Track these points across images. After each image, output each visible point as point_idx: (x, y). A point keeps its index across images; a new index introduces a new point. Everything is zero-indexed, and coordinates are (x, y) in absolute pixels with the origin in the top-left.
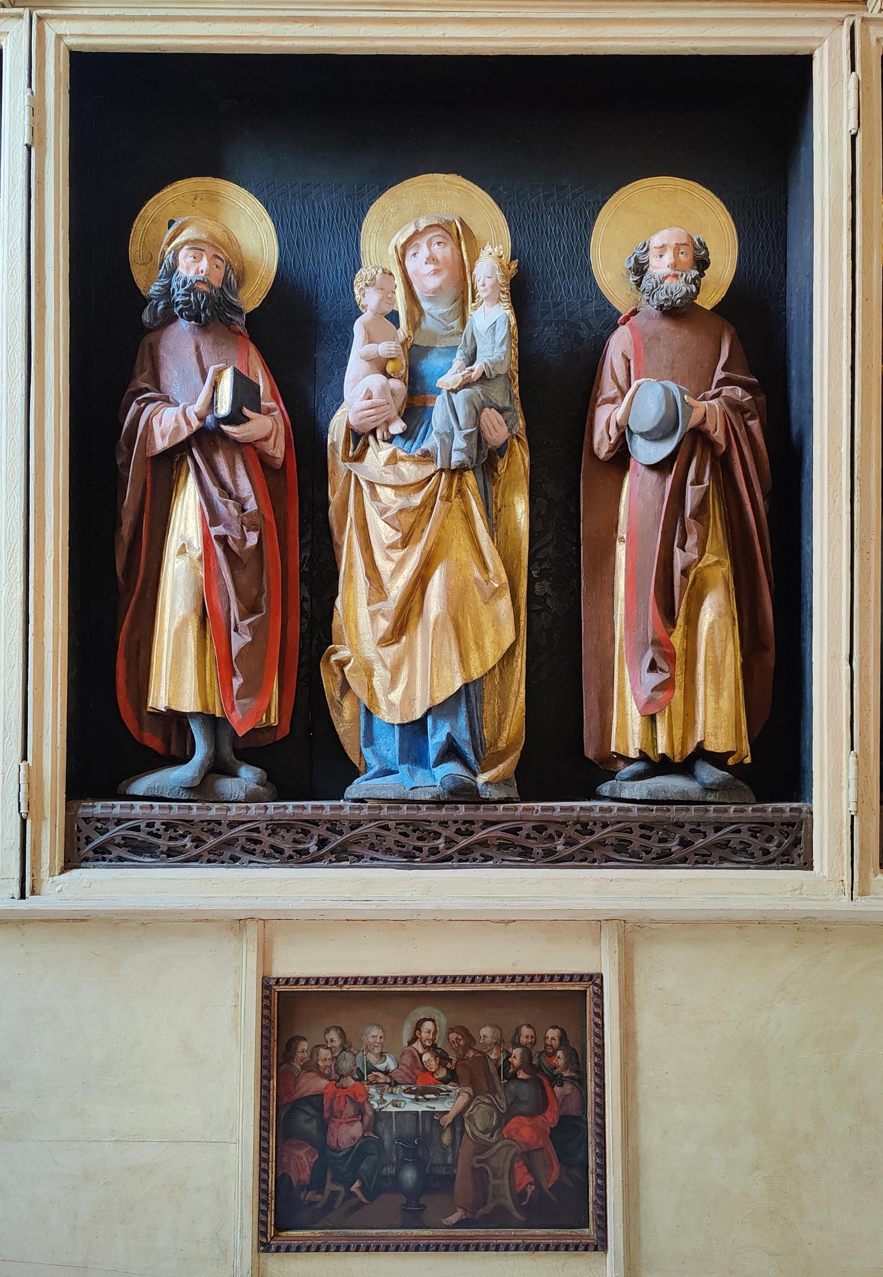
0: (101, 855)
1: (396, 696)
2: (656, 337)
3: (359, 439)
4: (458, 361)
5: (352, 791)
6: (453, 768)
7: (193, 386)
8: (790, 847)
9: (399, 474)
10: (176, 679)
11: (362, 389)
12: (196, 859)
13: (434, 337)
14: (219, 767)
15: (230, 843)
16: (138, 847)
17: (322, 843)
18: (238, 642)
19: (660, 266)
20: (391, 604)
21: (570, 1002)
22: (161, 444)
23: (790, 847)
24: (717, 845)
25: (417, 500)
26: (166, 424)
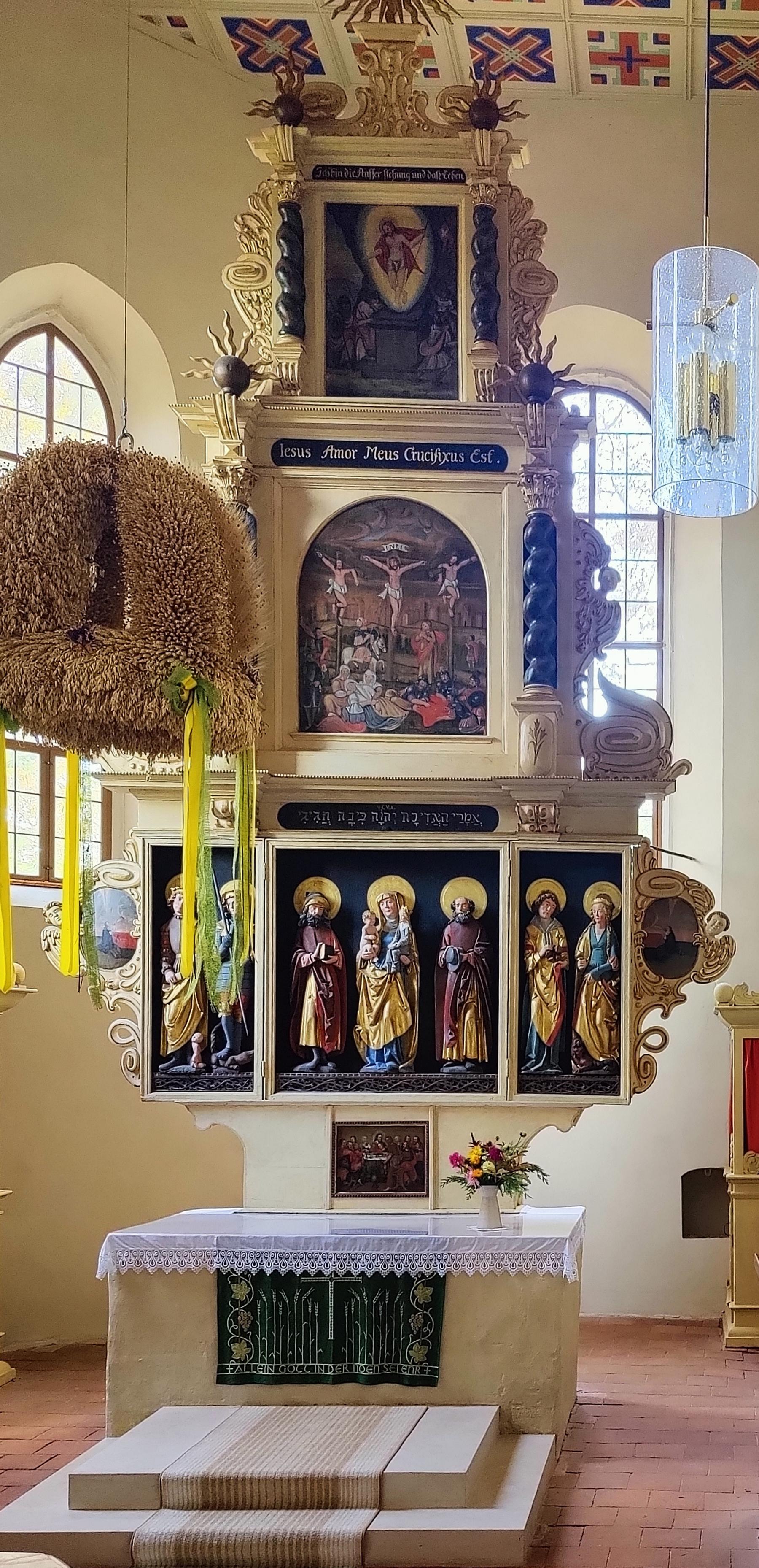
0: (285, 1089)
1: (375, 1041)
2: (458, 930)
3: (364, 961)
4: (395, 939)
5: (362, 1071)
6: (391, 1063)
7: (314, 950)
8: (492, 1087)
9: (375, 974)
10: (308, 1037)
11: (364, 949)
12: (314, 1090)
13: (389, 928)
14: (321, 1063)
15: (324, 1085)
16: (297, 1087)
17: (352, 1085)
18: (326, 1026)
19: (458, 910)
20: (373, 1014)
22: (303, 966)
23: (492, 1087)
24: (470, 1086)
25: (381, 982)
26: (305, 959)
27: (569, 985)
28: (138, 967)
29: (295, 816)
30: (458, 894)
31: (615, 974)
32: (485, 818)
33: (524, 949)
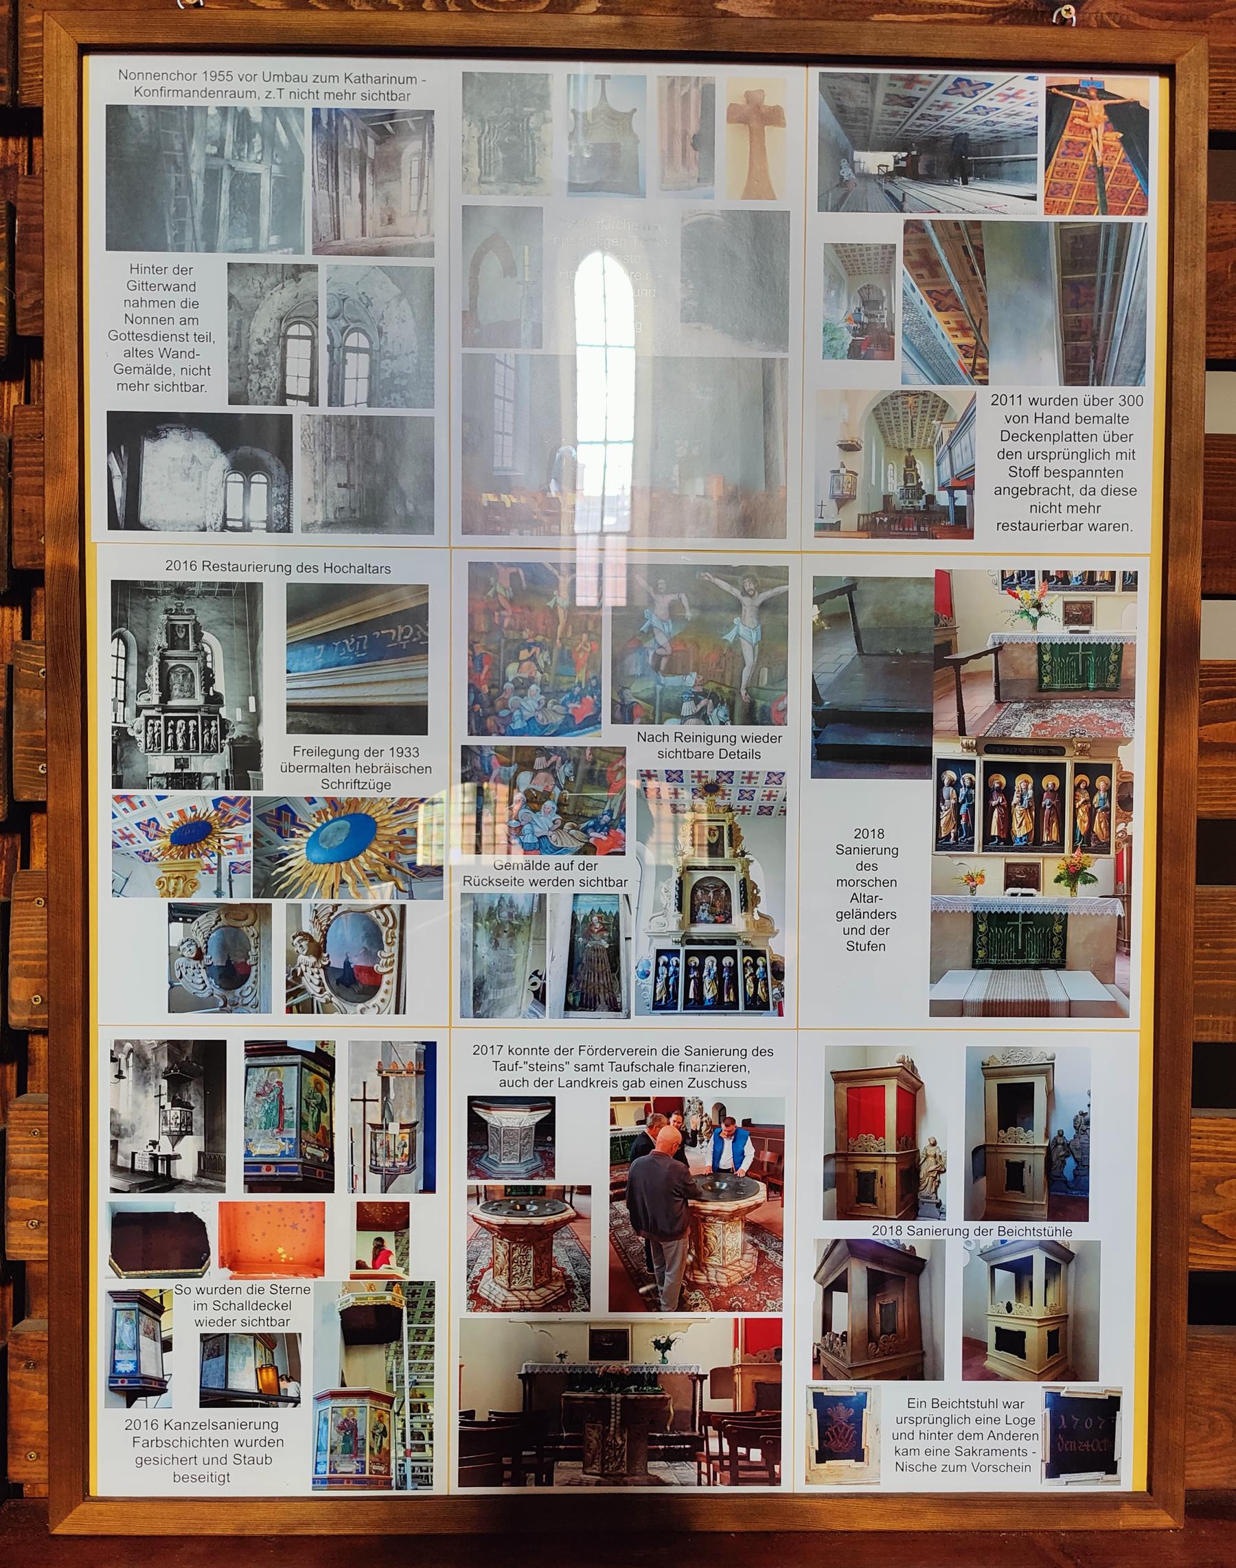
7: (997, 800)
10: (994, 831)
11: (1016, 799)
21: (1037, 865)
26: (994, 803)
27: (1092, 813)
29: (990, 749)
31: (1109, 809)
32: (1060, 751)
33: (1075, 800)
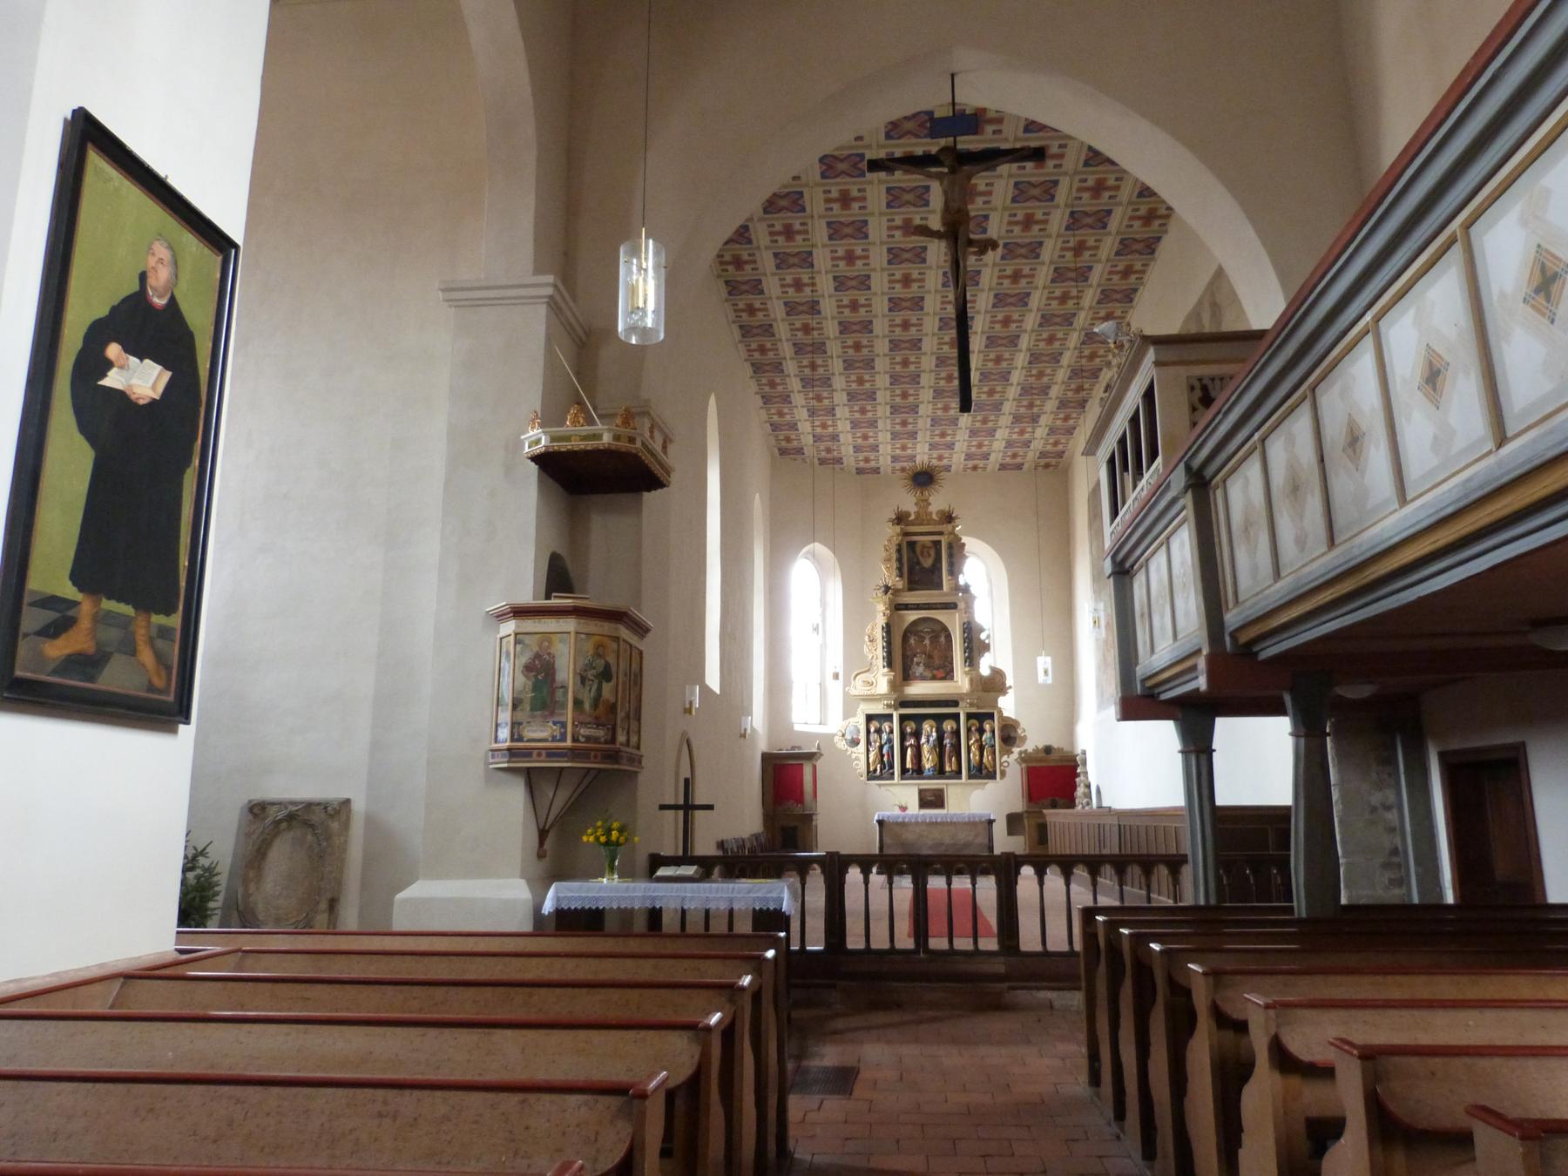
10: (909, 765)
11: (923, 740)
21: (941, 791)
27: (981, 749)
28: (862, 746)
30: (948, 726)
32: (955, 704)
33: (968, 739)
